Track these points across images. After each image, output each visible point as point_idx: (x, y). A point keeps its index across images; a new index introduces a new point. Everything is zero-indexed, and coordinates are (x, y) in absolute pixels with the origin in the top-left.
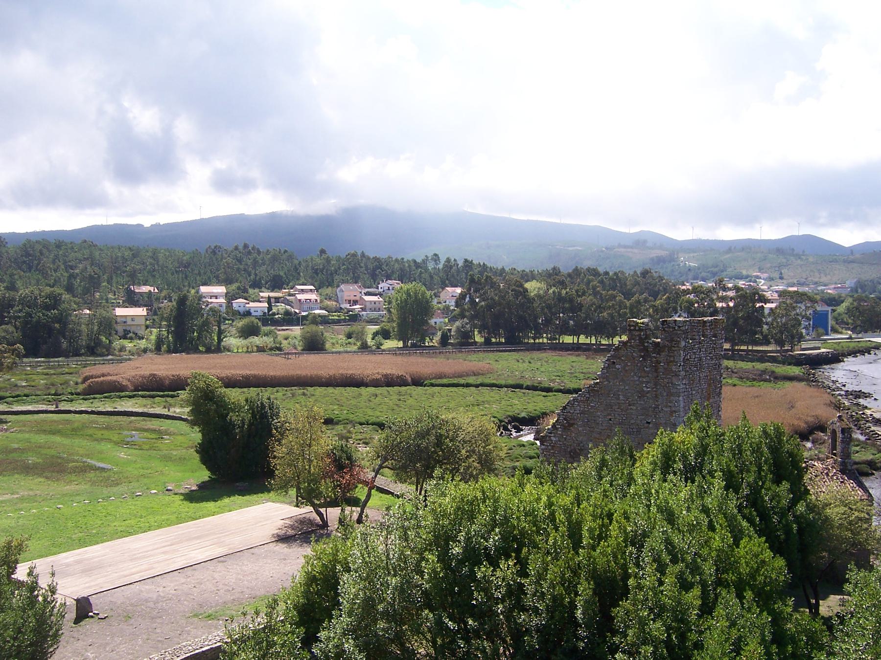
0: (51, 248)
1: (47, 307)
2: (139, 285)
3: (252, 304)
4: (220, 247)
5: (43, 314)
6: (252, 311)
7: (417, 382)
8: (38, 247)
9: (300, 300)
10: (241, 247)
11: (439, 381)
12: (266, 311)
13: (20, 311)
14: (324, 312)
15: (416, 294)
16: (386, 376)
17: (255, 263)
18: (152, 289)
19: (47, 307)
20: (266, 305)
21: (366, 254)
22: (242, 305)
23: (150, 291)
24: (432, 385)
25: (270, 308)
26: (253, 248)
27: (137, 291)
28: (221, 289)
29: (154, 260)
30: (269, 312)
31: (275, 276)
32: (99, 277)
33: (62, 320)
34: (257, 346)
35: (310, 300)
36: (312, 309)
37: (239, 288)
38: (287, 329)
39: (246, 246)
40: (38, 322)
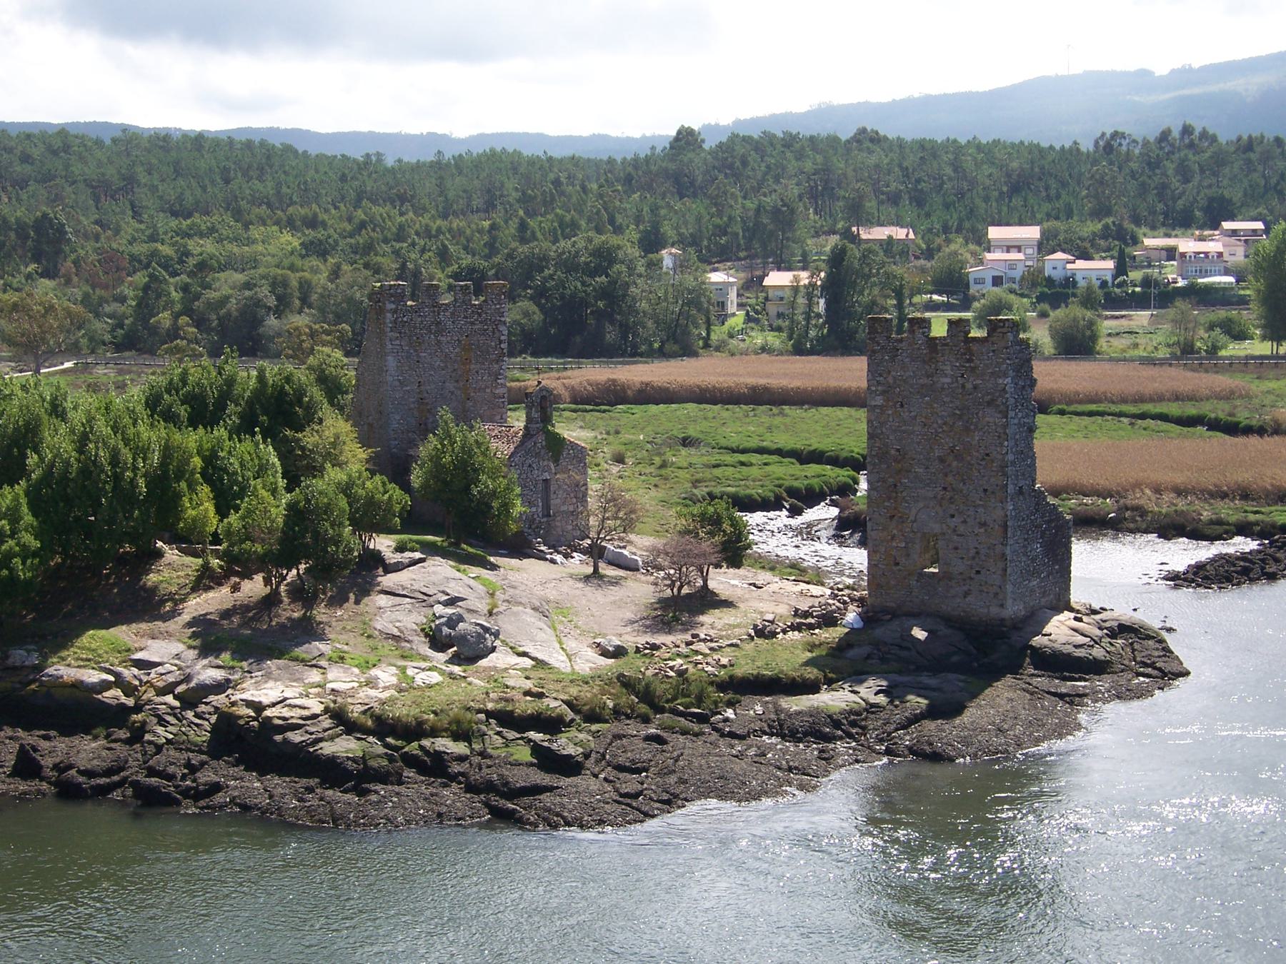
0: (769, 150)
3: (1081, 264)
4: (1123, 136)
5: (583, 284)
6: (1079, 278)
8: (740, 150)
9: (1183, 255)
10: (1176, 134)
11: (1080, 408)
12: (1109, 278)
13: (551, 277)
14: (1231, 279)
17: (1184, 173)
18: (900, 233)
19: (594, 273)
20: (1110, 264)
22: (1059, 265)
23: (890, 237)
25: (1121, 269)
27: (864, 236)
28: (1032, 233)
29: (955, 170)
30: (1115, 277)
31: (1211, 200)
32: (792, 211)
33: (614, 296)
35: (1206, 254)
36: (1206, 273)
37: (1106, 227)
38: (1122, 317)
39: (1187, 130)
40: (573, 296)
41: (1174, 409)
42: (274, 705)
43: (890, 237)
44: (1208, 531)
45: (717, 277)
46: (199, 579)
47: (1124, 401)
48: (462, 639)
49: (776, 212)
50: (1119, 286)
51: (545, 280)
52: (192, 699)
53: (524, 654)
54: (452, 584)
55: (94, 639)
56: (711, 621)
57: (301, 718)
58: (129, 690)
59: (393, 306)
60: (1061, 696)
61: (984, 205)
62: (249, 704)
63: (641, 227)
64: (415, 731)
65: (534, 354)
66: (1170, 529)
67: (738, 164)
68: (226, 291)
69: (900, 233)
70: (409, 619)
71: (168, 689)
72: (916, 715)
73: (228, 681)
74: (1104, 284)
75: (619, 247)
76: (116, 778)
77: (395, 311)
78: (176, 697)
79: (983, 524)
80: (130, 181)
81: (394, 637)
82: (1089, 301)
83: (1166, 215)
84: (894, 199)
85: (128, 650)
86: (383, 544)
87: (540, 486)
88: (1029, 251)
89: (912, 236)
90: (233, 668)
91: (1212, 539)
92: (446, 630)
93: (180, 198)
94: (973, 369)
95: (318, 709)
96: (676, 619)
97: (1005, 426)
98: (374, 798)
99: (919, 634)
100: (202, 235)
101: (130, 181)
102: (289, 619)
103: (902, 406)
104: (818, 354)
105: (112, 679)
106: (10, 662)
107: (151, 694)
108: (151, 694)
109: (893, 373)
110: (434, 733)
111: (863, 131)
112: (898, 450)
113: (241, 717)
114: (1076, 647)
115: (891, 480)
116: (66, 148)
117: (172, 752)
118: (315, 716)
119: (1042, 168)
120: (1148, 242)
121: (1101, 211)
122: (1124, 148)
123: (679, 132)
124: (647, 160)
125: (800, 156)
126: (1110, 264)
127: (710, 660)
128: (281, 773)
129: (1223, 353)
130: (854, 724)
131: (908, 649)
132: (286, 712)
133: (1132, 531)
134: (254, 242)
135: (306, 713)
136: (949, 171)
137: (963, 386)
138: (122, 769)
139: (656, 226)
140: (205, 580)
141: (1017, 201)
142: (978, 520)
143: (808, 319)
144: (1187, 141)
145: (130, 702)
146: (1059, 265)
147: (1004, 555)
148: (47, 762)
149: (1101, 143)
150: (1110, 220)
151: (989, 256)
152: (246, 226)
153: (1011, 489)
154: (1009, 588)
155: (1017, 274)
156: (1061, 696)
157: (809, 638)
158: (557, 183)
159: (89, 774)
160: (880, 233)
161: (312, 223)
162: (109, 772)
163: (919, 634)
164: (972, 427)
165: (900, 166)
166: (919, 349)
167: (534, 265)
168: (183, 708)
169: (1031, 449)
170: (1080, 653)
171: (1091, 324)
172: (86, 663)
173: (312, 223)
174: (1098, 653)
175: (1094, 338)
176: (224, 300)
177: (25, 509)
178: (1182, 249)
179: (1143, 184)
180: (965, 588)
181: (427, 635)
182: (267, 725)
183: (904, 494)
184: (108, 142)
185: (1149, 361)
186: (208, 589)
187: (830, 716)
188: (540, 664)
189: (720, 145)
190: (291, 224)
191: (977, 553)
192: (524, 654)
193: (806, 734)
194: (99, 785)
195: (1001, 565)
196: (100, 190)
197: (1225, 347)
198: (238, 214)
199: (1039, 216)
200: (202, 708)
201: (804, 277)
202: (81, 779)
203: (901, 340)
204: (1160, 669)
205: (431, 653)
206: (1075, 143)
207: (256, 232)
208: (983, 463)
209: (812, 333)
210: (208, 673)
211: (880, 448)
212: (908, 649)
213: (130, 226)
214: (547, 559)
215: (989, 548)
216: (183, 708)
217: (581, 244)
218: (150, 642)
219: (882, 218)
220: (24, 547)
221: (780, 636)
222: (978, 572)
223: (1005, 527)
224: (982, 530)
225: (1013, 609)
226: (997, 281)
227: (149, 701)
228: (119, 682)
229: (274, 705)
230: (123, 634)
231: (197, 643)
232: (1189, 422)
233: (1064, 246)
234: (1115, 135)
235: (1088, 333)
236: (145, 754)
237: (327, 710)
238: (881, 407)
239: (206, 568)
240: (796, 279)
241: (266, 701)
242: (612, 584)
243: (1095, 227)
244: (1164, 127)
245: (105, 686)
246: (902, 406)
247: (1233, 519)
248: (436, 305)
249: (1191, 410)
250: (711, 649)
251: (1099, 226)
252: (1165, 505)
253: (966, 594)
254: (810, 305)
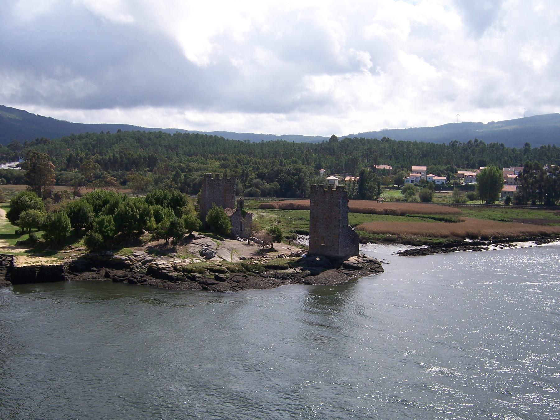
1: (294, 175)
2: (379, 164)
3: (436, 178)
5: (291, 178)
6: (436, 181)
7: (403, 214)
9: (466, 176)
10: (473, 142)
11: (413, 215)
12: (444, 182)
15: (490, 173)
16: (386, 210)
18: (387, 167)
19: (294, 175)
20: (445, 178)
21: (556, 147)
24: (408, 216)
25: (448, 179)
26: (481, 142)
27: (377, 168)
28: (424, 168)
30: (446, 182)
32: (357, 160)
33: (300, 181)
34: (396, 199)
35: (472, 176)
37: (448, 167)
38: (446, 193)
39: (476, 141)
41: (437, 216)
42: (161, 264)
43: (384, 168)
44: (416, 244)
45: (332, 178)
46: (151, 239)
47: (426, 214)
48: (207, 254)
49: (352, 160)
50: (447, 184)
51: (281, 176)
52: (145, 263)
53: (221, 258)
54: (209, 242)
55: (125, 250)
56: (270, 254)
57: (166, 267)
58: (131, 261)
59: (208, 179)
60: (347, 274)
61: (415, 160)
62: (155, 264)
63: (316, 163)
64: (191, 271)
65: (276, 197)
66: (406, 243)
67: (346, 146)
68: (195, 177)
69: (387, 167)
70: (197, 249)
71: (140, 261)
72: (307, 275)
73: (153, 260)
74: (443, 183)
75: (302, 168)
76: (125, 278)
77: (208, 180)
78: (141, 263)
79: (334, 234)
80: (177, 146)
81: (193, 253)
82: (430, 188)
83: (468, 165)
84: (390, 157)
85: (132, 252)
86: (196, 234)
87: (240, 223)
88: (423, 173)
89: (391, 168)
90: (154, 257)
91: (416, 245)
92: (204, 252)
93: (190, 151)
95: (170, 265)
96: (262, 253)
97: (340, 211)
98: (177, 284)
99: (318, 259)
100: (194, 162)
101: (177, 146)
102: (170, 248)
104: (355, 199)
105: (128, 258)
106: (106, 254)
107: (136, 262)
108: (136, 262)
110: (195, 272)
111: (384, 138)
113: (153, 267)
114: (354, 263)
116: (160, 136)
117: (138, 274)
118: (169, 267)
119: (433, 150)
120: (459, 172)
121: (447, 164)
122: (458, 145)
123: (332, 137)
124: (321, 144)
125: (364, 145)
126: (445, 178)
127: (264, 261)
128: (160, 279)
129: (467, 203)
130: (292, 276)
131: (314, 262)
132: (163, 266)
133: (398, 243)
134: (208, 164)
135: (167, 266)
136: (405, 150)
138: (127, 276)
139: (320, 164)
140: (152, 239)
141: (425, 159)
143: (353, 190)
144: (476, 144)
145: (131, 263)
146: (431, 178)
147: (338, 241)
148: (111, 275)
149: (451, 144)
150: (449, 166)
151: (411, 174)
152: (206, 160)
153: (341, 226)
154: (340, 249)
155: (418, 180)
156: (347, 274)
157: (291, 259)
158: (295, 150)
159: (119, 277)
160: (382, 167)
161: (225, 159)
162: (124, 277)
163: (318, 259)
165: (393, 148)
167: (278, 173)
168: (142, 265)
169: (347, 217)
170: (355, 265)
171: (431, 194)
172: (123, 255)
173: (225, 159)
174: (360, 265)
175: (431, 198)
176: (195, 179)
177: (112, 221)
178: (465, 175)
179: (461, 156)
181: (200, 253)
182: (159, 269)
184: (172, 135)
185: (448, 205)
186: (153, 241)
187: (287, 274)
188: (224, 260)
189: (342, 141)
190: (219, 159)
192: (221, 258)
193: (281, 278)
194: (121, 279)
195: (338, 244)
196: (168, 148)
197: (468, 201)
198: (204, 156)
199: (430, 164)
200: (146, 265)
201: (353, 179)
202: (118, 278)
203: (318, 190)
204: (375, 270)
205: (200, 257)
206: (444, 143)
207: (208, 161)
209: (354, 194)
210: (149, 258)
212: (314, 262)
213: (175, 158)
214: (239, 240)
216: (142, 265)
217: (292, 167)
218: (138, 251)
219: (385, 163)
220: (111, 229)
221: (284, 258)
222: (333, 245)
223: (339, 235)
225: (341, 254)
226: (413, 181)
227: (135, 263)
228: (130, 259)
229: (161, 264)
230: (132, 249)
231: (147, 252)
232: (441, 220)
233: (433, 172)
234: (456, 142)
235: (429, 196)
236: (132, 274)
237: (172, 266)
239: (153, 236)
240: (351, 179)
241: (159, 263)
242: (251, 246)
243: (445, 167)
244: (469, 140)
245: (126, 260)
247: (423, 241)
248: (218, 179)
249: (441, 216)
250: (266, 259)
251: (446, 167)
252: (409, 237)
254: (354, 186)
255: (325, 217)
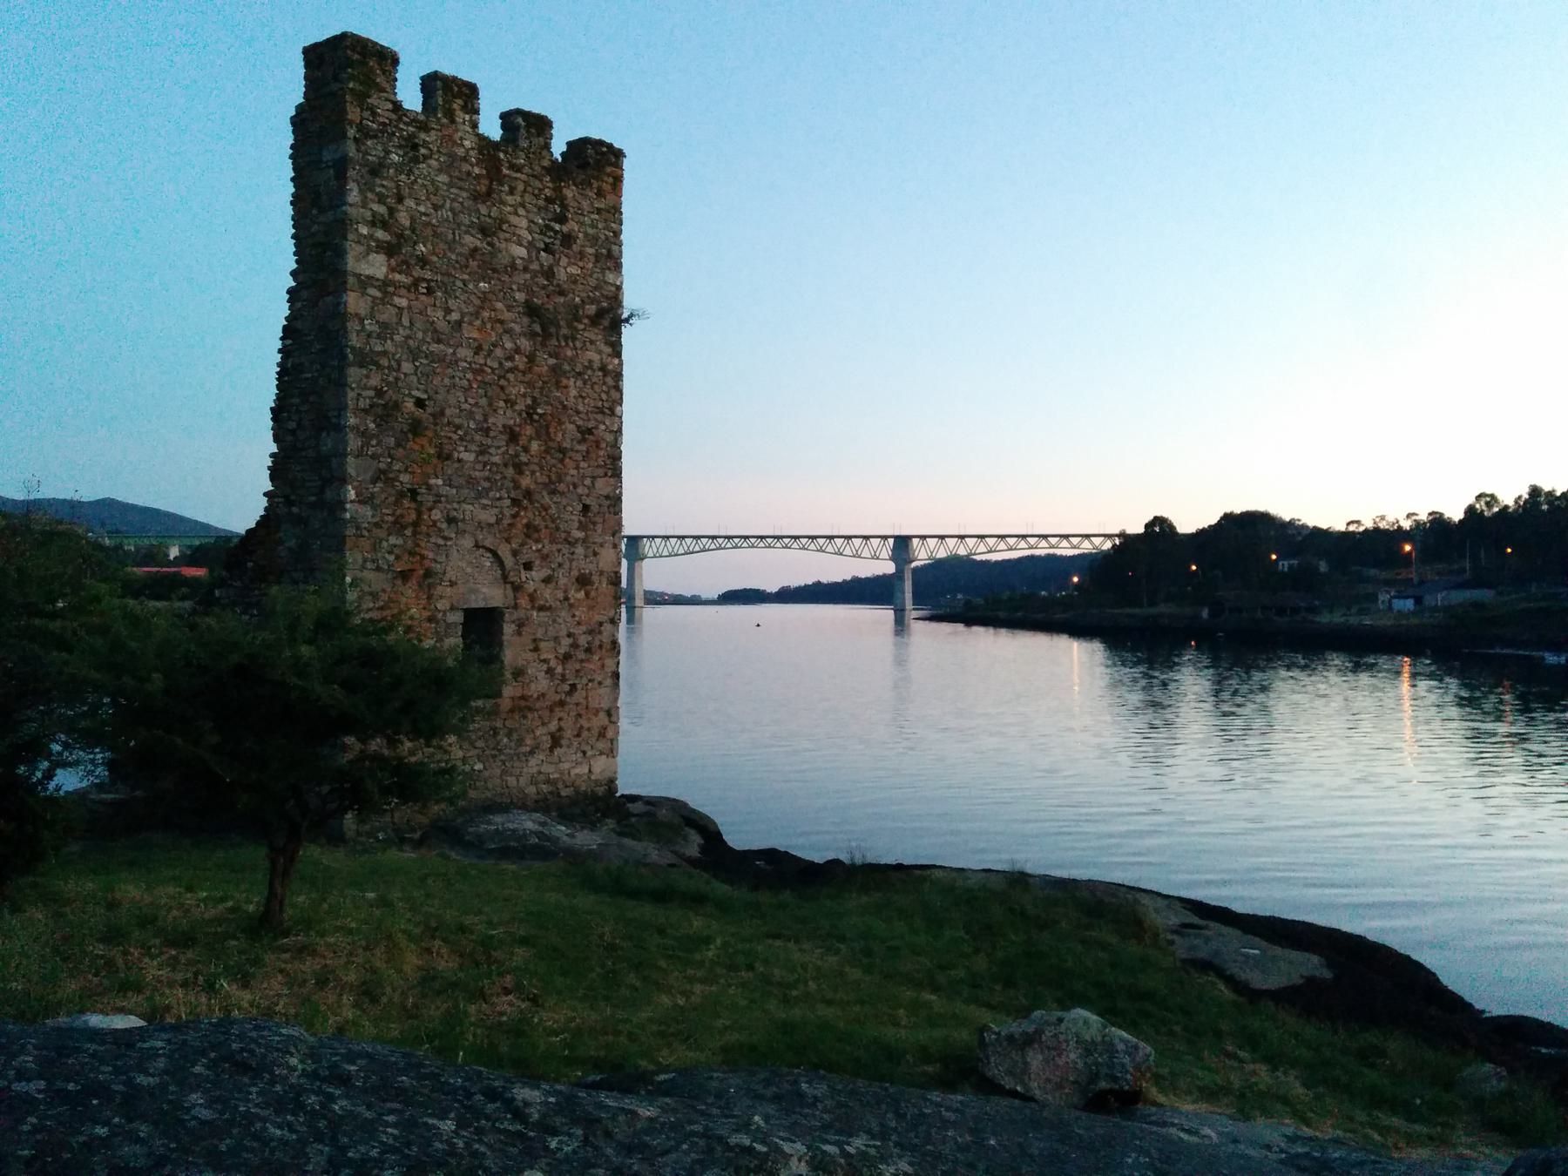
94: (568, 240)
103: (430, 292)
109: (410, 203)
112: (420, 403)
115: (404, 478)
137: (549, 274)
142: (575, 573)
164: (567, 367)
166: (465, 159)
180: (553, 726)
183: (437, 515)
191: (575, 646)
208: (583, 448)
211: (379, 393)
215: (590, 632)
224: (581, 595)
238: (384, 284)
246: (430, 292)
253: (556, 741)
255: (500, 420)
